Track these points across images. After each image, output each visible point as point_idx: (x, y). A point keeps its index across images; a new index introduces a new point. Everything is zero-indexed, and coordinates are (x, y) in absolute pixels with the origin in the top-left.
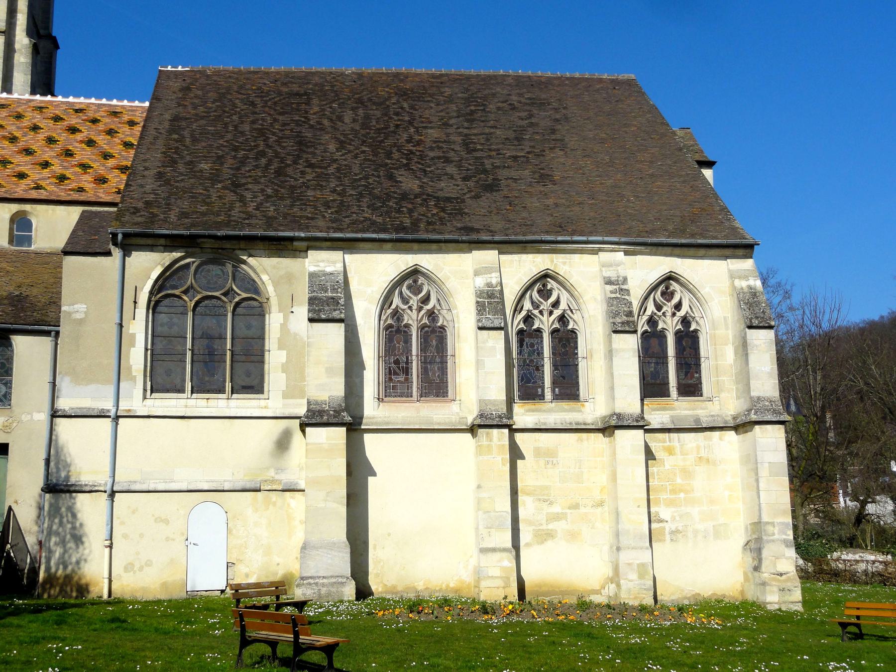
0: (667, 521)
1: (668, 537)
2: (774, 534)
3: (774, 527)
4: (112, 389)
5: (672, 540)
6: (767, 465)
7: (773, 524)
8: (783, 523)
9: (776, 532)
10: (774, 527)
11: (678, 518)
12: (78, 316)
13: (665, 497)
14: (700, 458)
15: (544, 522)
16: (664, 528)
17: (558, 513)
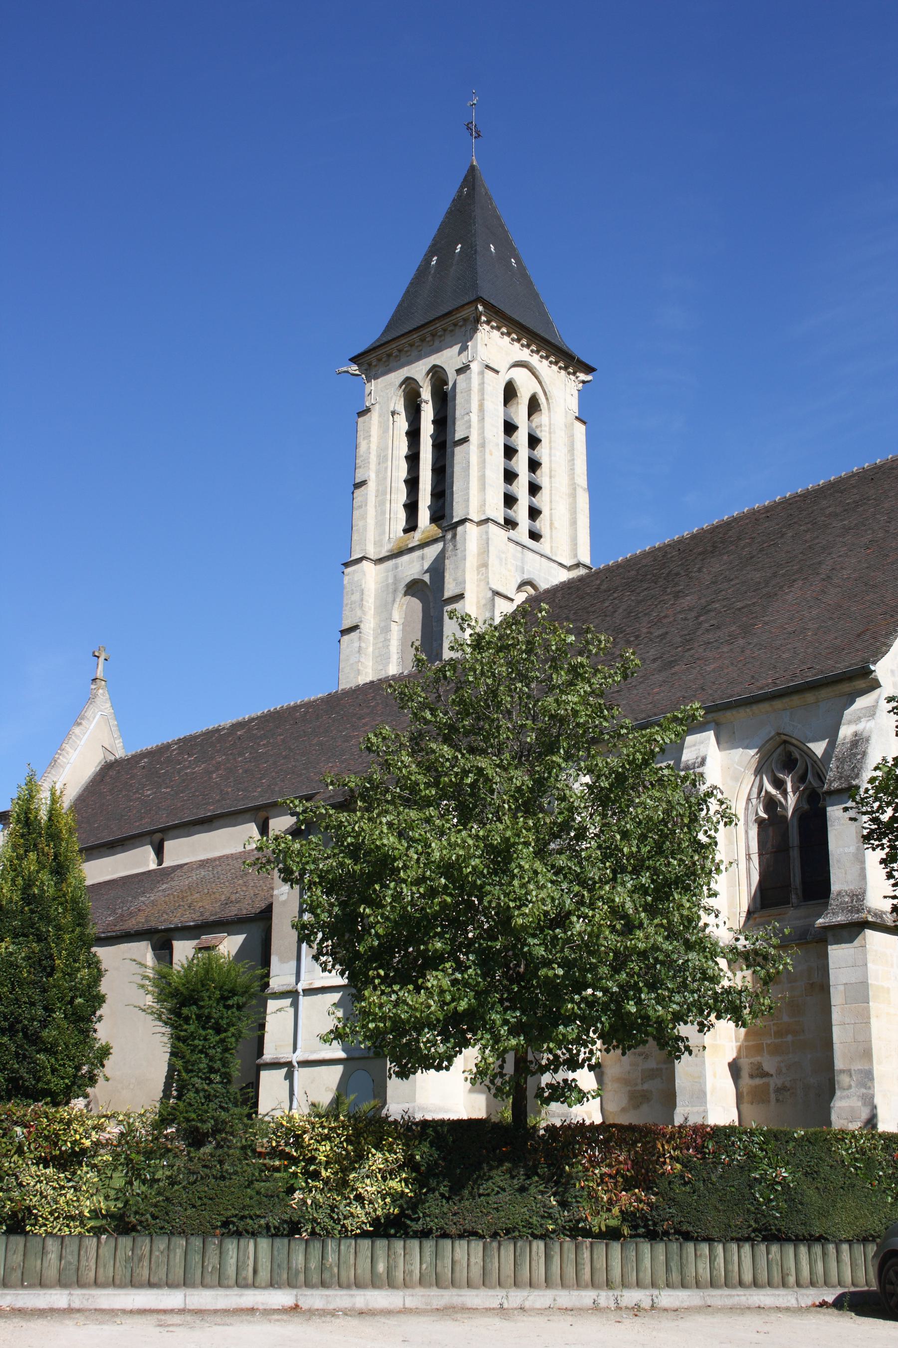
0: (772, 1075)
1: (773, 1096)
2: (850, 1087)
3: (851, 1076)
4: (294, 963)
5: (778, 1100)
6: (841, 988)
7: (849, 1072)
8: (860, 1071)
9: (853, 1084)
10: (851, 1076)
11: (784, 1070)
12: (283, 898)
13: (769, 1042)
14: (812, 984)
15: (639, 1081)
16: (768, 1085)
17: (652, 1070)
